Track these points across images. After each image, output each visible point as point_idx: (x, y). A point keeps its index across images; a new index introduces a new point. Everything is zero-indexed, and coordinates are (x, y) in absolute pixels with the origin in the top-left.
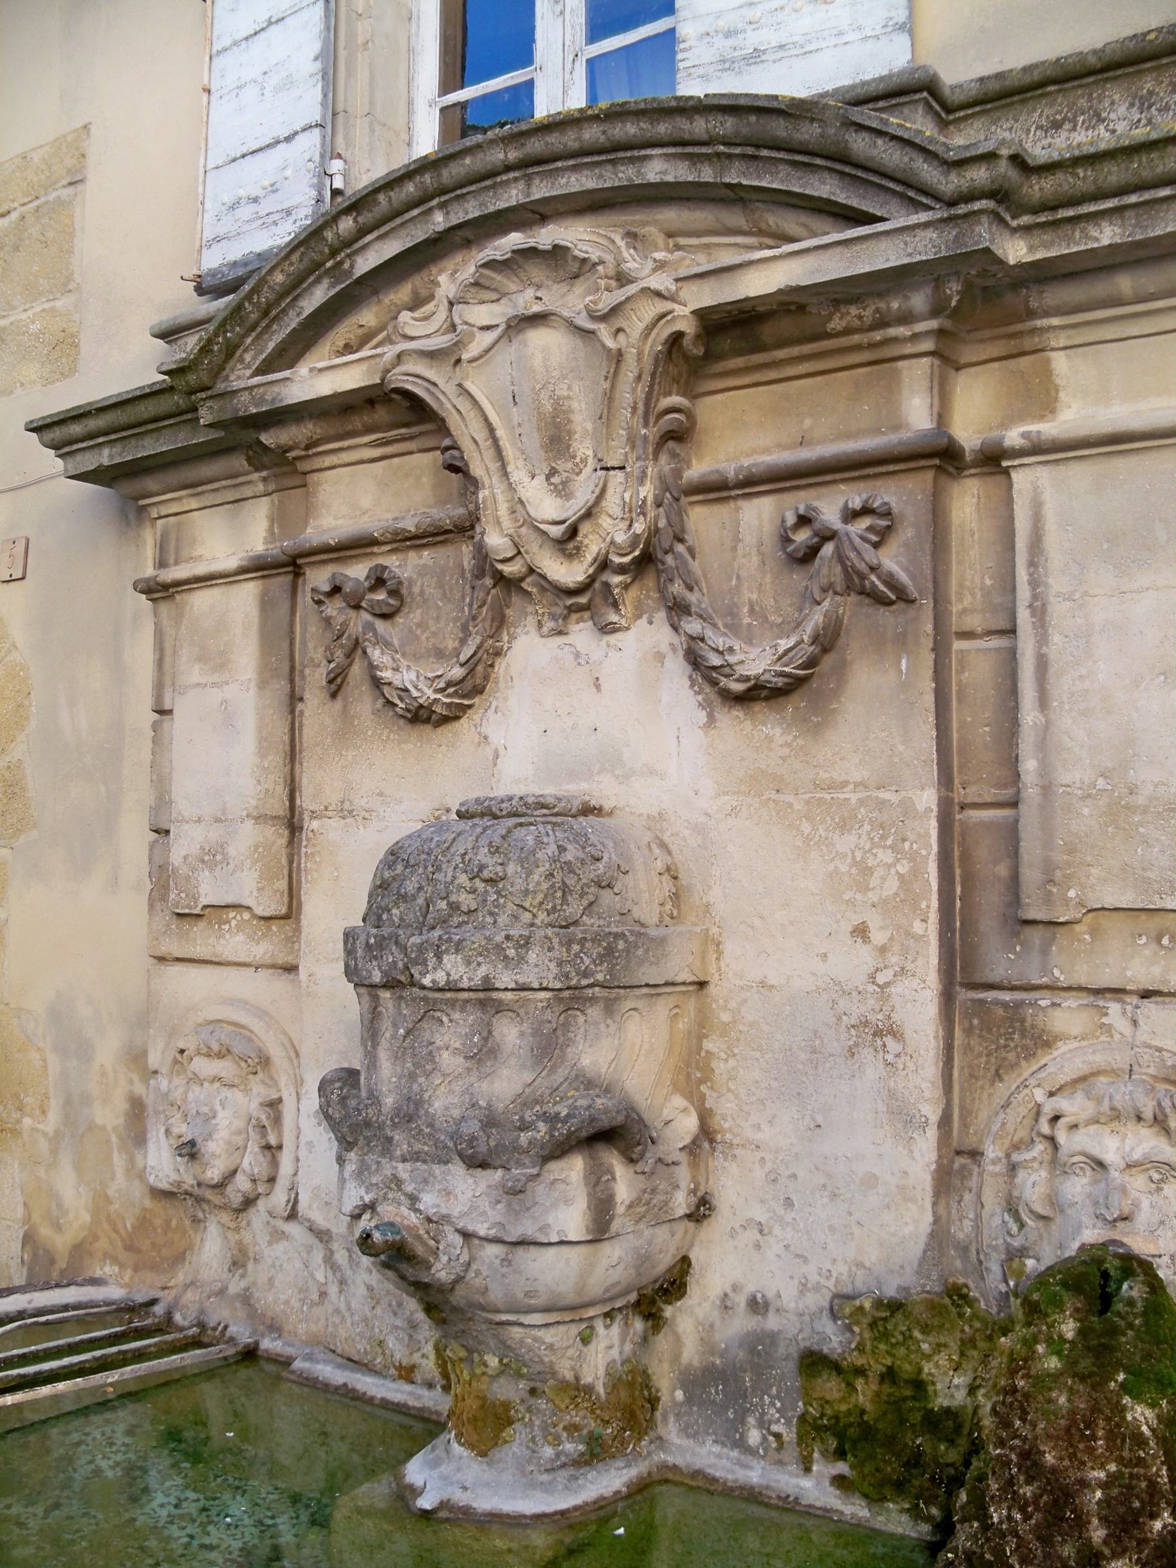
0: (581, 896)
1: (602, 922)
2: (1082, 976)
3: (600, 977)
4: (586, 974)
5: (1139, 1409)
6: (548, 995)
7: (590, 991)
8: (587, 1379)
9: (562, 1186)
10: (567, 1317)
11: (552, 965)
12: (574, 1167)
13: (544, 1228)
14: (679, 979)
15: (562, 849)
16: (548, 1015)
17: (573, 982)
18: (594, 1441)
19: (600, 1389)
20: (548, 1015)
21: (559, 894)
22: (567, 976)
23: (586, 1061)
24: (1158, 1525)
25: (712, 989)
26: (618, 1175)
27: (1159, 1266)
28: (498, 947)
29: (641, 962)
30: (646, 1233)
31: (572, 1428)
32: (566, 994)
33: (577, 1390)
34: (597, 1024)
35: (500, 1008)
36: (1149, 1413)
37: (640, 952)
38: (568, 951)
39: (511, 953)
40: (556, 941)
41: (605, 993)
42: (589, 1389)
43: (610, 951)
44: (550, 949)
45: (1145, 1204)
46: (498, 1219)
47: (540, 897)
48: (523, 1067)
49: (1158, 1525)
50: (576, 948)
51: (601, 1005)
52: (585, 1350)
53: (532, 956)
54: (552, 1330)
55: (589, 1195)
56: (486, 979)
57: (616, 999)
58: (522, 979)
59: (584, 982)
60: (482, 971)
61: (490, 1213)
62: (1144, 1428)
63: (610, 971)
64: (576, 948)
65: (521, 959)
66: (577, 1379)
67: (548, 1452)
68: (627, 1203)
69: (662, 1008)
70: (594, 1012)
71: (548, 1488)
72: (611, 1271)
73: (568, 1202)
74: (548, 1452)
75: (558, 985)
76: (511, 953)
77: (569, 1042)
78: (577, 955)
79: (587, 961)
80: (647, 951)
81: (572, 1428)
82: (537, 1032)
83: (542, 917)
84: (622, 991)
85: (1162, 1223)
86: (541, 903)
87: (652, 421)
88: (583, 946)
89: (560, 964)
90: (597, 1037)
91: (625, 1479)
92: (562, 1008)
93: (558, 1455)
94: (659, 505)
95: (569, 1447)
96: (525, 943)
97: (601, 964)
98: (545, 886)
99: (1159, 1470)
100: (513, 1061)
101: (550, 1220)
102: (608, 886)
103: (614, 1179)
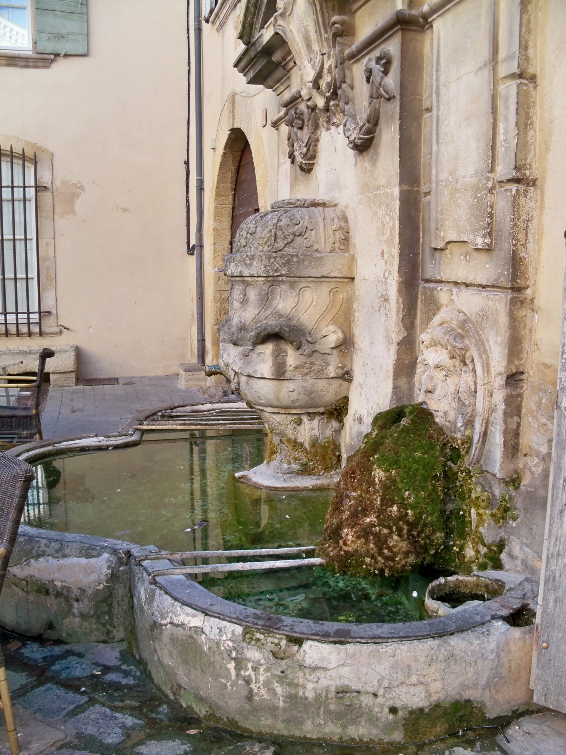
0: (283, 240)
1: (294, 250)
2: (314, 273)
3: (284, 272)
4: (276, 271)
5: (378, 471)
6: (263, 279)
7: (281, 278)
8: (300, 440)
9: (263, 355)
10: (282, 411)
11: (262, 267)
12: (268, 349)
13: (255, 371)
14: (332, 275)
15: (279, 220)
16: (264, 287)
17: (271, 274)
18: (305, 465)
19: (307, 445)
20: (264, 287)
21: (273, 239)
22: (268, 271)
23: (280, 307)
24: (368, 520)
25: (356, 281)
26: (289, 354)
27: (437, 416)
28: (244, 259)
29: (307, 267)
30: (310, 381)
31: (296, 459)
32: (270, 279)
33: (296, 444)
34: (285, 292)
35: (248, 284)
36: (382, 473)
37: (307, 263)
38: (269, 261)
39: (248, 262)
40: (264, 257)
41: (289, 279)
42: (301, 445)
43: (289, 262)
44: (261, 260)
45: (439, 386)
46: (241, 366)
47: (265, 240)
48: (255, 307)
49: (368, 520)
50: (272, 260)
51: (288, 284)
52: (298, 428)
53: (255, 263)
54: (279, 416)
55: (273, 360)
56: (241, 272)
57: (295, 282)
58: (252, 272)
59: (276, 274)
60: (240, 269)
61: (239, 363)
62: (377, 480)
63: (289, 270)
64: (272, 260)
65: (251, 264)
66: (295, 439)
67: (286, 466)
68: (293, 366)
69: (325, 288)
70: (284, 287)
71: (277, 479)
72: (290, 393)
73: (265, 361)
74: (286, 466)
75: (265, 275)
76: (248, 262)
77: (274, 298)
78: (272, 263)
79: (277, 266)
80: (310, 262)
81: (296, 459)
82: (260, 294)
83: (266, 248)
84: (298, 279)
85: (445, 396)
86: (266, 243)
87: (329, 29)
88: (275, 259)
89: (265, 266)
90: (286, 297)
91: (313, 483)
92: (270, 284)
93: (289, 468)
94: (336, 67)
95: (293, 466)
96: (252, 258)
97: (284, 266)
98: (268, 235)
99: (377, 498)
100: (252, 305)
101: (257, 368)
102: (300, 235)
103: (287, 355)
